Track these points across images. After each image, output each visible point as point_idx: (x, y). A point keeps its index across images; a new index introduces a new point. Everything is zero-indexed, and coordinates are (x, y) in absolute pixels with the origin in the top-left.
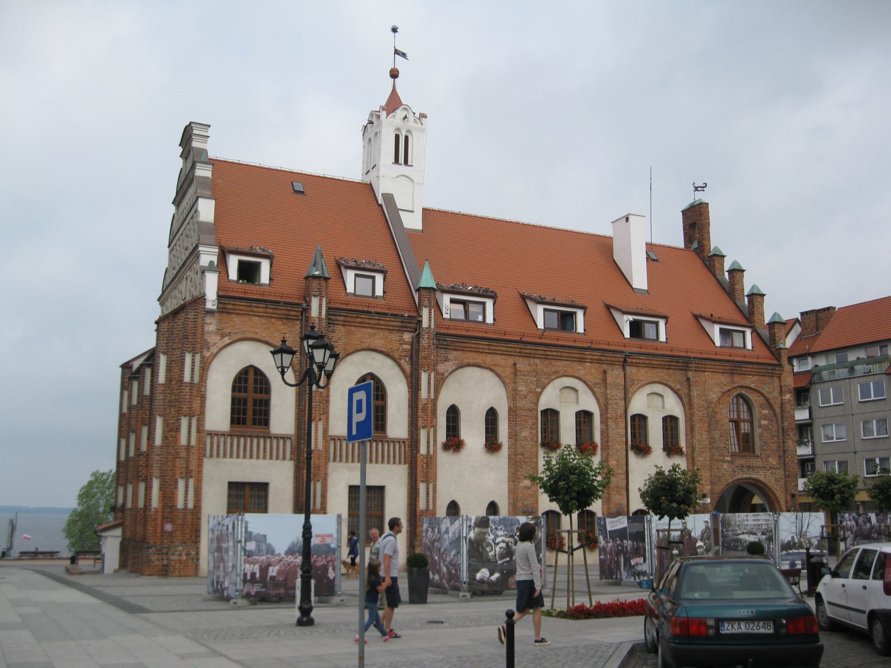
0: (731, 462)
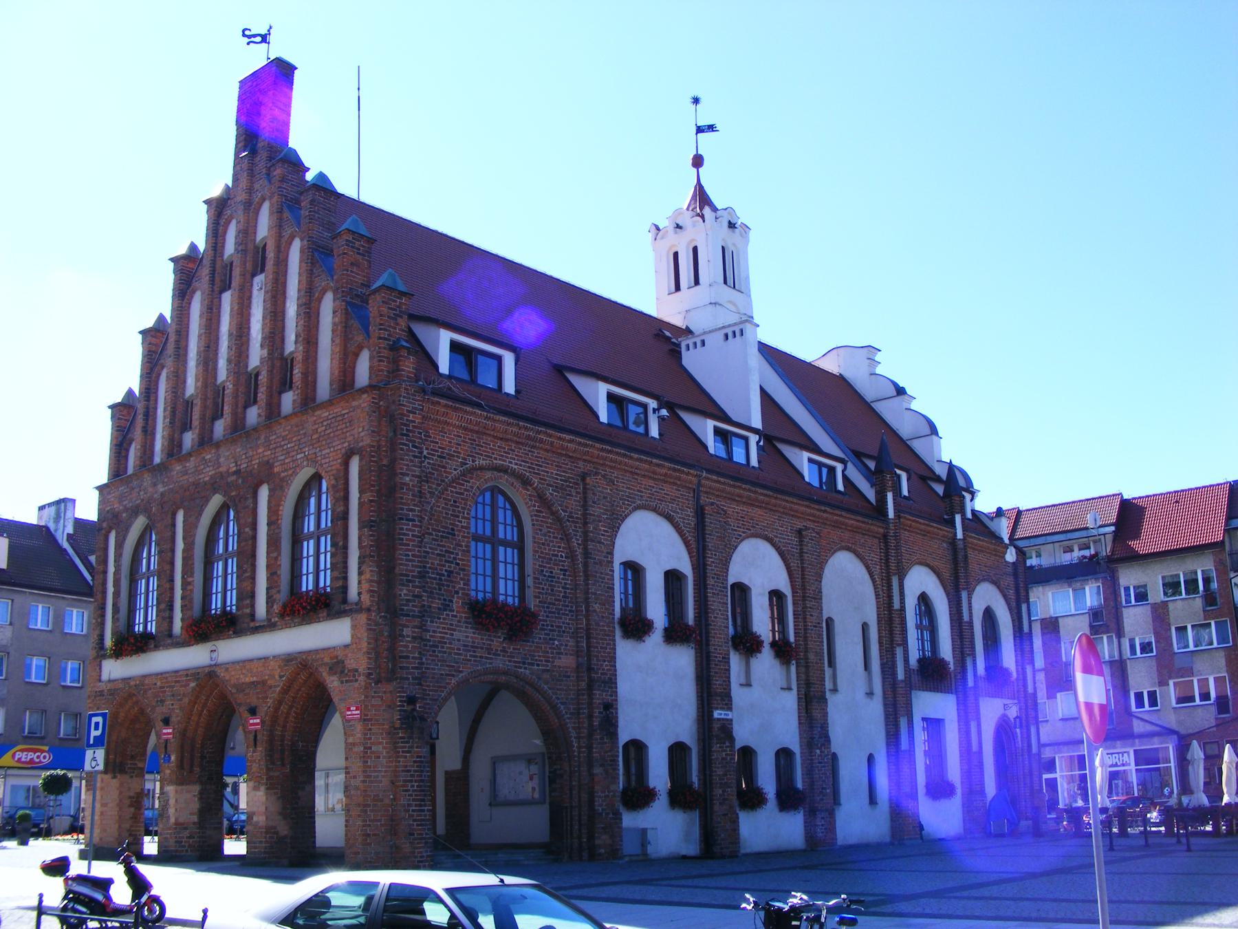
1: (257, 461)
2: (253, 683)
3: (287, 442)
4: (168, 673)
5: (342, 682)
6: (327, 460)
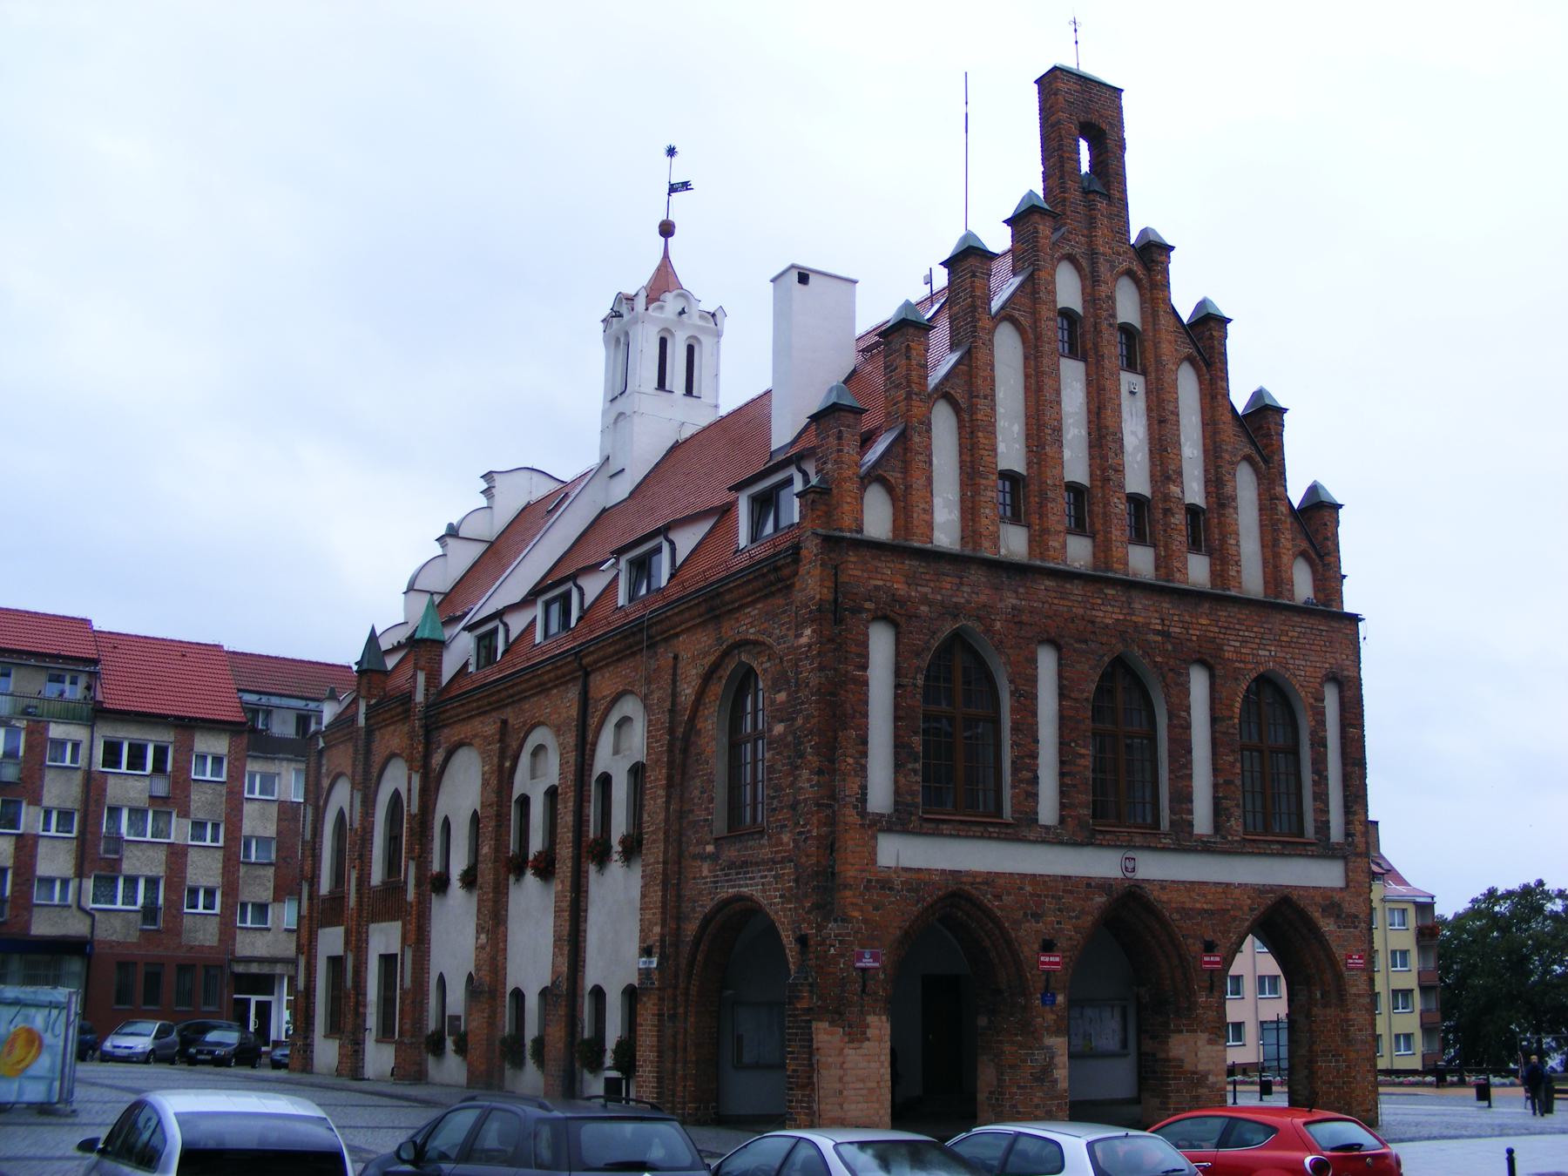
0: (714, 857)
1: (1198, 633)
2: (1206, 911)
3: (1244, 628)
4: (1049, 876)
5: (1339, 927)
6: (1303, 673)
